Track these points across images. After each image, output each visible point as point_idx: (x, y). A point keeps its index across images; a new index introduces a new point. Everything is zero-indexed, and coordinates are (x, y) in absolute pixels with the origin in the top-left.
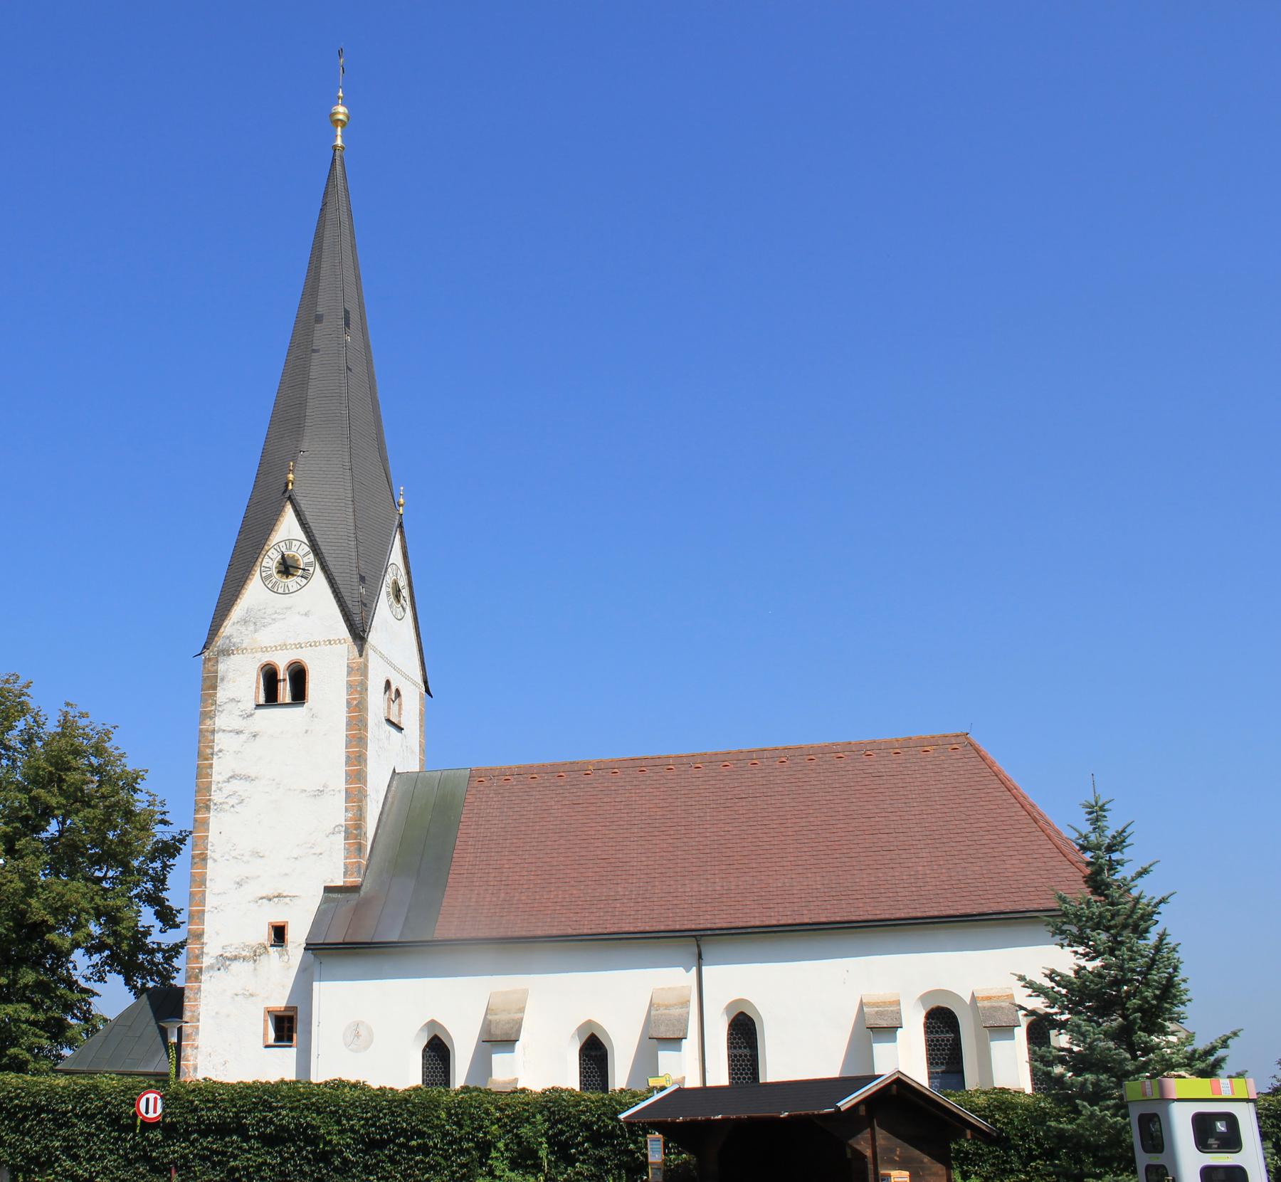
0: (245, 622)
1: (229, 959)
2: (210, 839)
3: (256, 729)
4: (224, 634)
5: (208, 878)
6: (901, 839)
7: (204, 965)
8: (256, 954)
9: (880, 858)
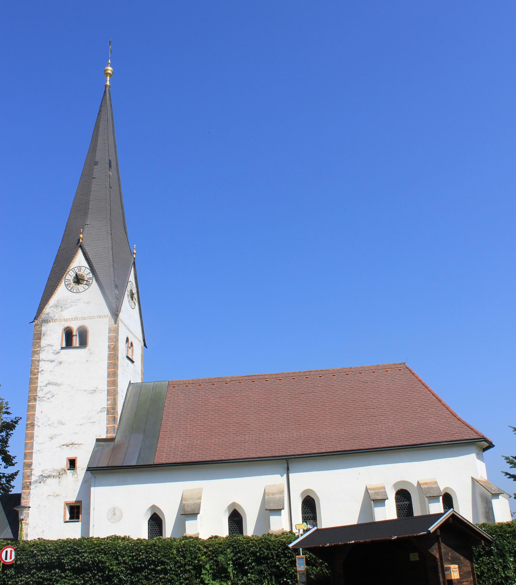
0: (56, 306)
2: (36, 415)
3: (60, 360)
4: (45, 312)
6: (380, 411)
7: (32, 481)
8: (60, 474)
9: (371, 420)
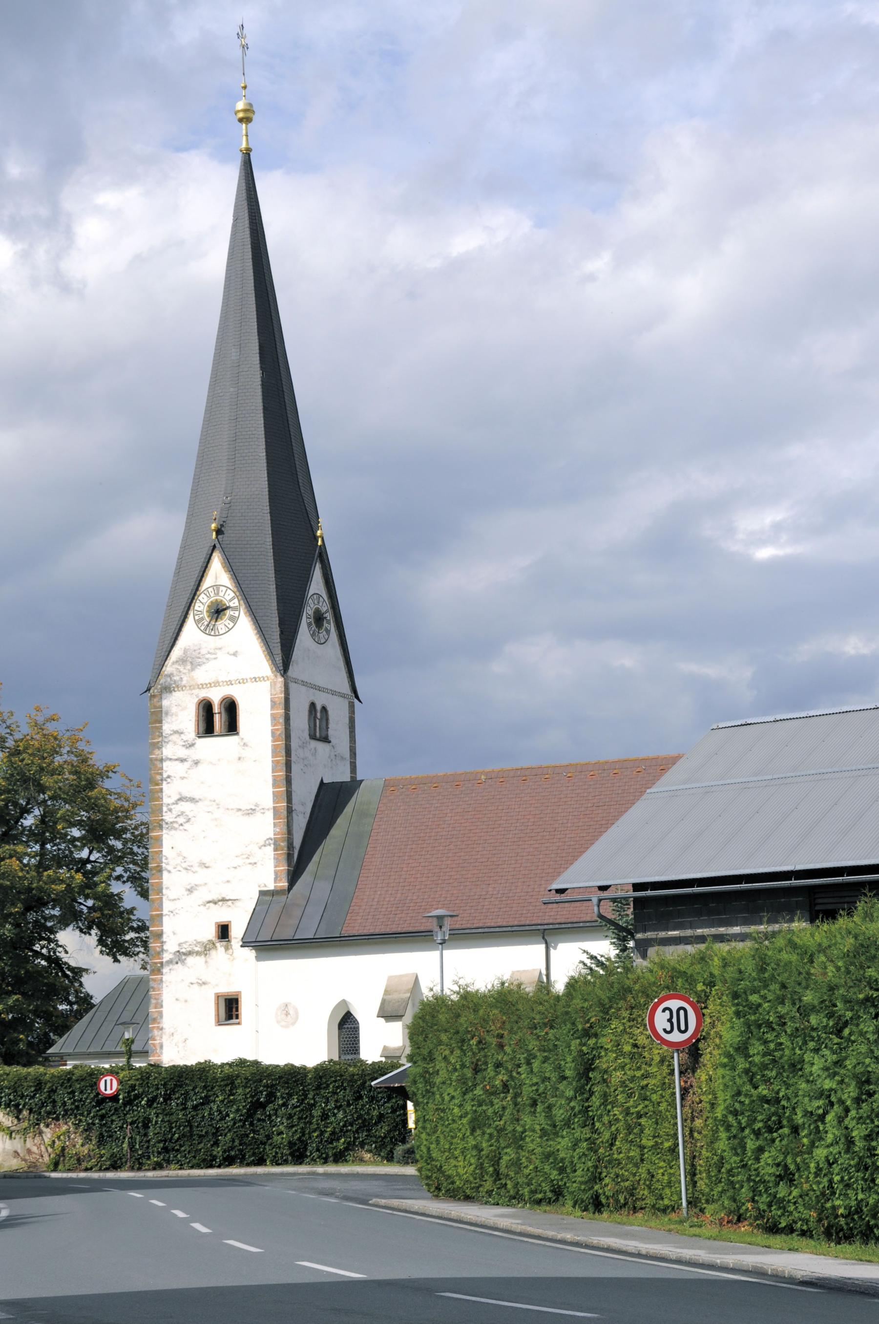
1: (184, 954)
2: (164, 853)
3: (195, 757)
4: (166, 673)
5: (164, 887)
7: (164, 960)
